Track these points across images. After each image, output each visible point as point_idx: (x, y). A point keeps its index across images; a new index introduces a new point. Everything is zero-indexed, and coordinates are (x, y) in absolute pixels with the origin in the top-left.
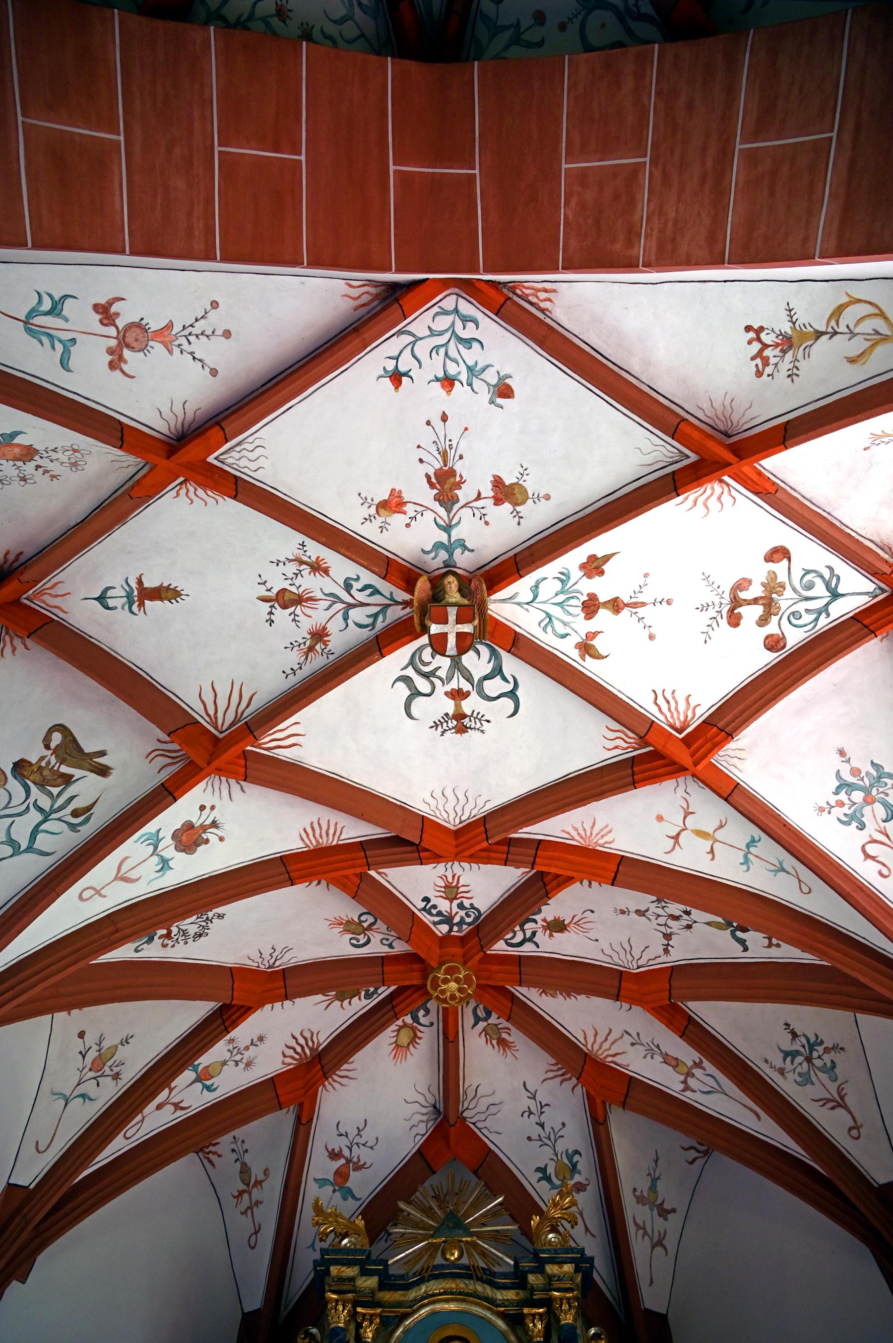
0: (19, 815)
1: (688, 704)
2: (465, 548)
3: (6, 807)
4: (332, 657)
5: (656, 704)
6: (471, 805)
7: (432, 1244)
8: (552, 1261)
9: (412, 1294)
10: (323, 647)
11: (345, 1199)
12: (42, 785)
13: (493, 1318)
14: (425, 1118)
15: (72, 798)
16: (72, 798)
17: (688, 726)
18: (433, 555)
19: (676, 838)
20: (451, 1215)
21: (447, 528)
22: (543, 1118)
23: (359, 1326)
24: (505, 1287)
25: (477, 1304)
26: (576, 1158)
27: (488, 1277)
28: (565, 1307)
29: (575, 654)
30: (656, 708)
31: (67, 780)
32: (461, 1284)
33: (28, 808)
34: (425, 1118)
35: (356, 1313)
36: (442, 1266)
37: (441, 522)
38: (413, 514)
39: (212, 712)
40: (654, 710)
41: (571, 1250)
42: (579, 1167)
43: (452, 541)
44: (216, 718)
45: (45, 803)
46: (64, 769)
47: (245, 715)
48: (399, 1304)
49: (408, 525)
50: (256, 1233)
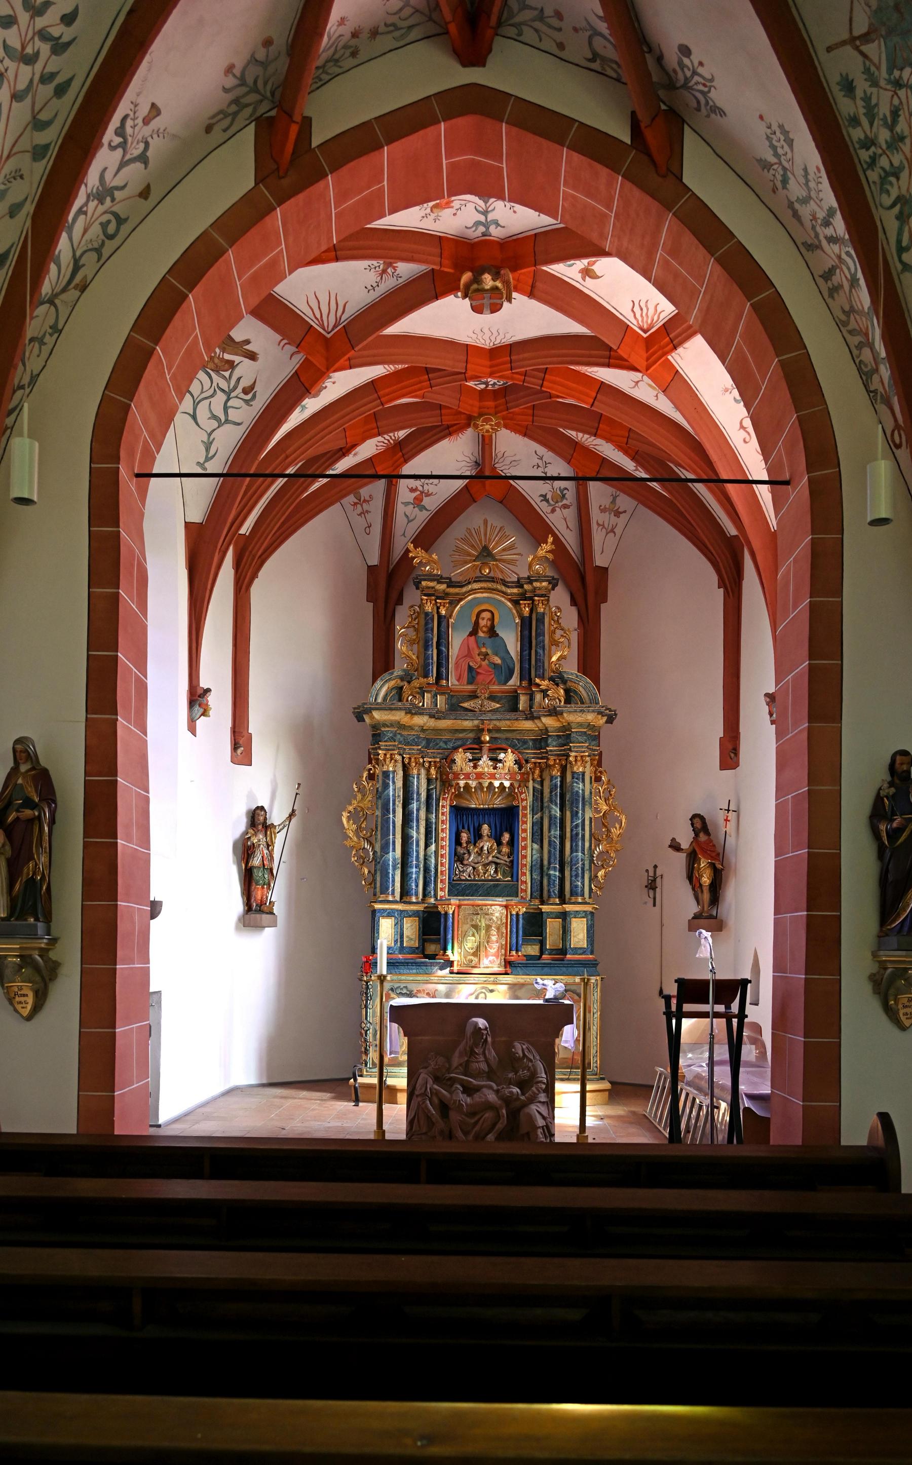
0: (212, 396)
1: (656, 310)
2: (497, 224)
3: (202, 392)
4: (400, 280)
5: (633, 311)
6: (502, 336)
7: (474, 565)
8: (536, 581)
9: (464, 590)
10: (393, 271)
11: (421, 511)
12: (217, 370)
13: (506, 601)
14: (470, 468)
15: (239, 379)
16: (239, 379)
17: (653, 327)
18: (474, 229)
19: (637, 383)
20: (485, 548)
21: (485, 213)
22: (546, 470)
23: (438, 608)
24: (512, 587)
25: (498, 595)
26: (565, 492)
27: (504, 583)
28: (540, 605)
29: (579, 277)
30: (633, 315)
31: (231, 365)
32: (490, 585)
33: (215, 390)
34: (470, 468)
35: (436, 602)
36: (480, 577)
37: (480, 209)
38: (458, 207)
39: (318, 316)
40: (630, 316)
41: (548, 577)
42: (566, 496)
43: (488, 220)
44: (322, 320)
45: (224, 385)
46: (227, 357)
47: (342, 320)
48: (457, 594)
49: (455, 214)
50: (369, 527)
